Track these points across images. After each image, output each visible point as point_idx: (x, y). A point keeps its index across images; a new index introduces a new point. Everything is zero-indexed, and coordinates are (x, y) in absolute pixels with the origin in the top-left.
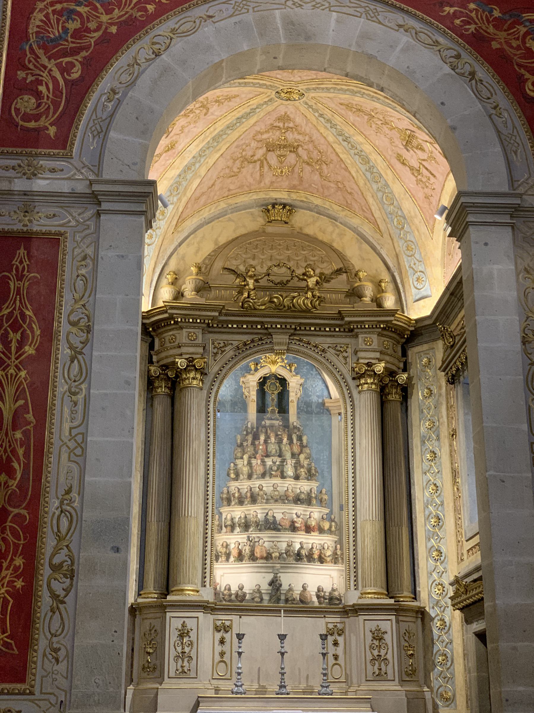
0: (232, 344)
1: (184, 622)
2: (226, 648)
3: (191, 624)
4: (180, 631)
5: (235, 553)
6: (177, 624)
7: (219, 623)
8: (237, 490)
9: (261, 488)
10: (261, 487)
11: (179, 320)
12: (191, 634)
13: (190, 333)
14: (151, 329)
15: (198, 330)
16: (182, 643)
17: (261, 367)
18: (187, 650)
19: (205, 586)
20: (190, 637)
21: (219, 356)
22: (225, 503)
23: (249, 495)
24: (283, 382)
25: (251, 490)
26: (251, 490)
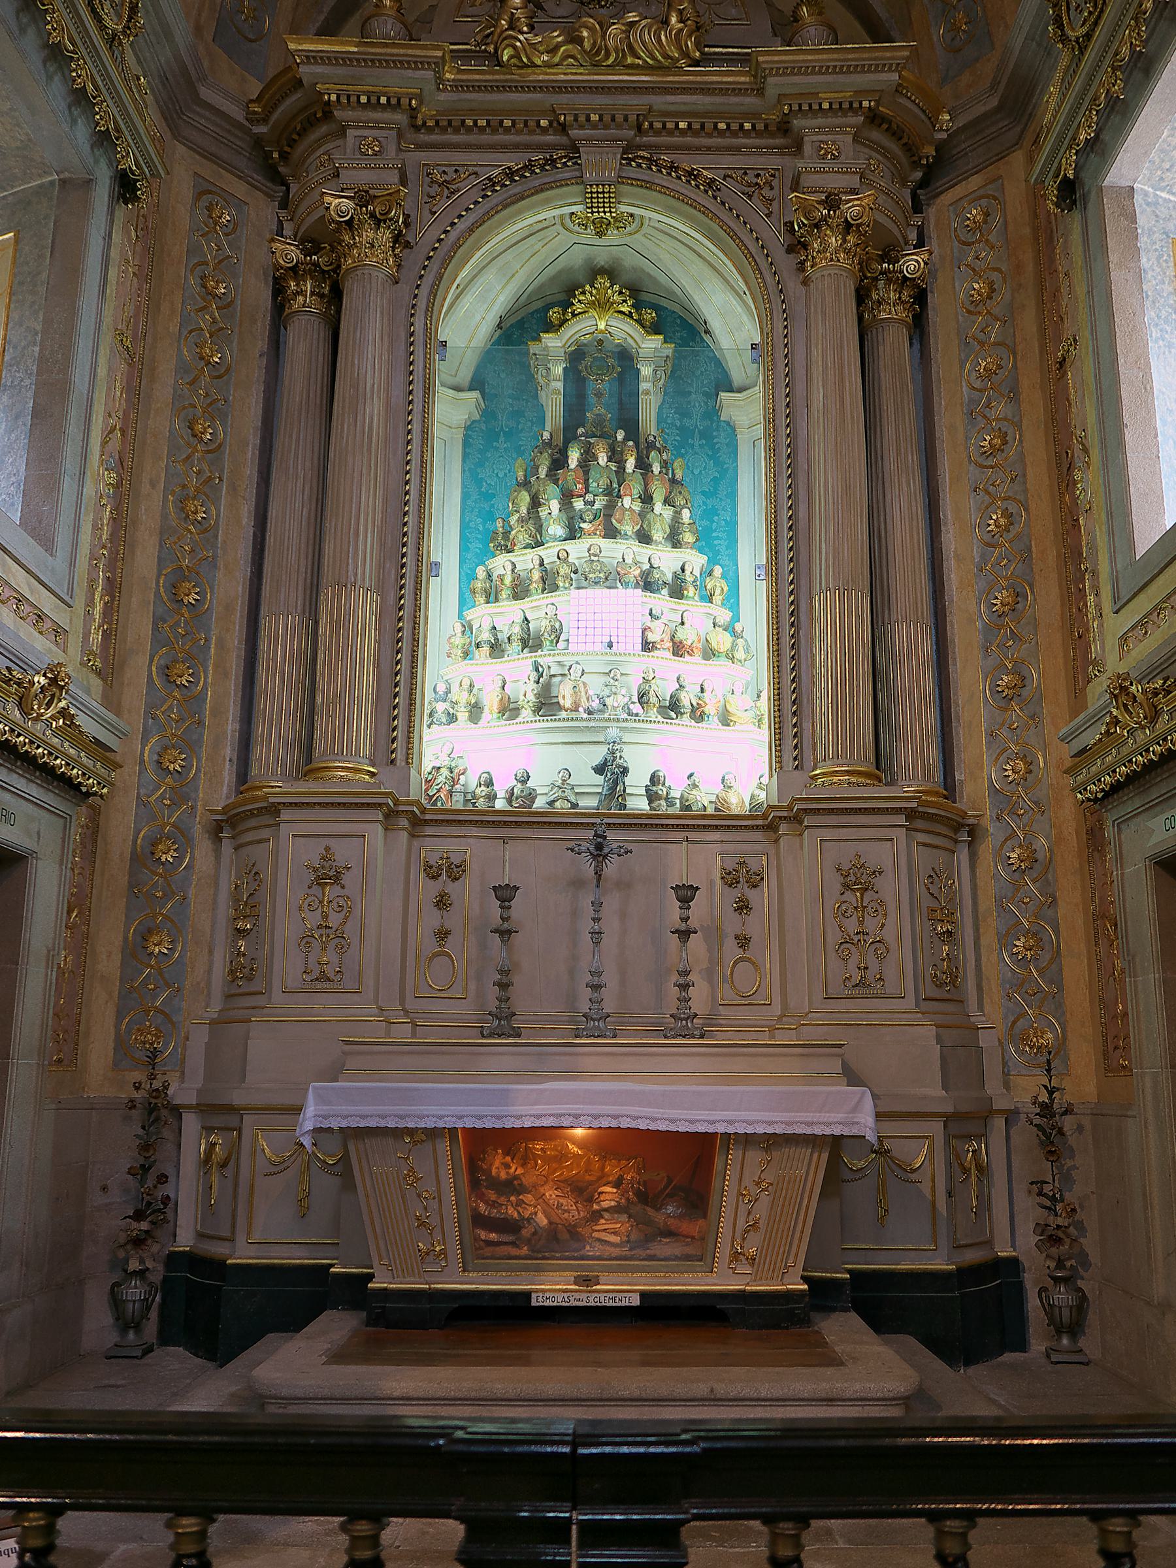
0: (476, 173)
1: (327, 849)
2: (452, 920)
3: (343, 853)
4: (315, 870)
5: (491, 702)
6: (312, 853)
7: (434, 859)
8: (509, 567)
9: (563, 558)
10: (563, 555)
11: (333, 97)
12: (346, 879)
13: (366, 137)
14: (276, 155)
15: (384, 133)
16: (321, 902)
17: (574, 315)
18: (334, 920)
19: (393, 762)
20: (343, 887)
21: (442, 205)
22: (482, 599)
23: (536, 575)
24: (626, 358)
25: (542, 564)
26: (542, 564)
